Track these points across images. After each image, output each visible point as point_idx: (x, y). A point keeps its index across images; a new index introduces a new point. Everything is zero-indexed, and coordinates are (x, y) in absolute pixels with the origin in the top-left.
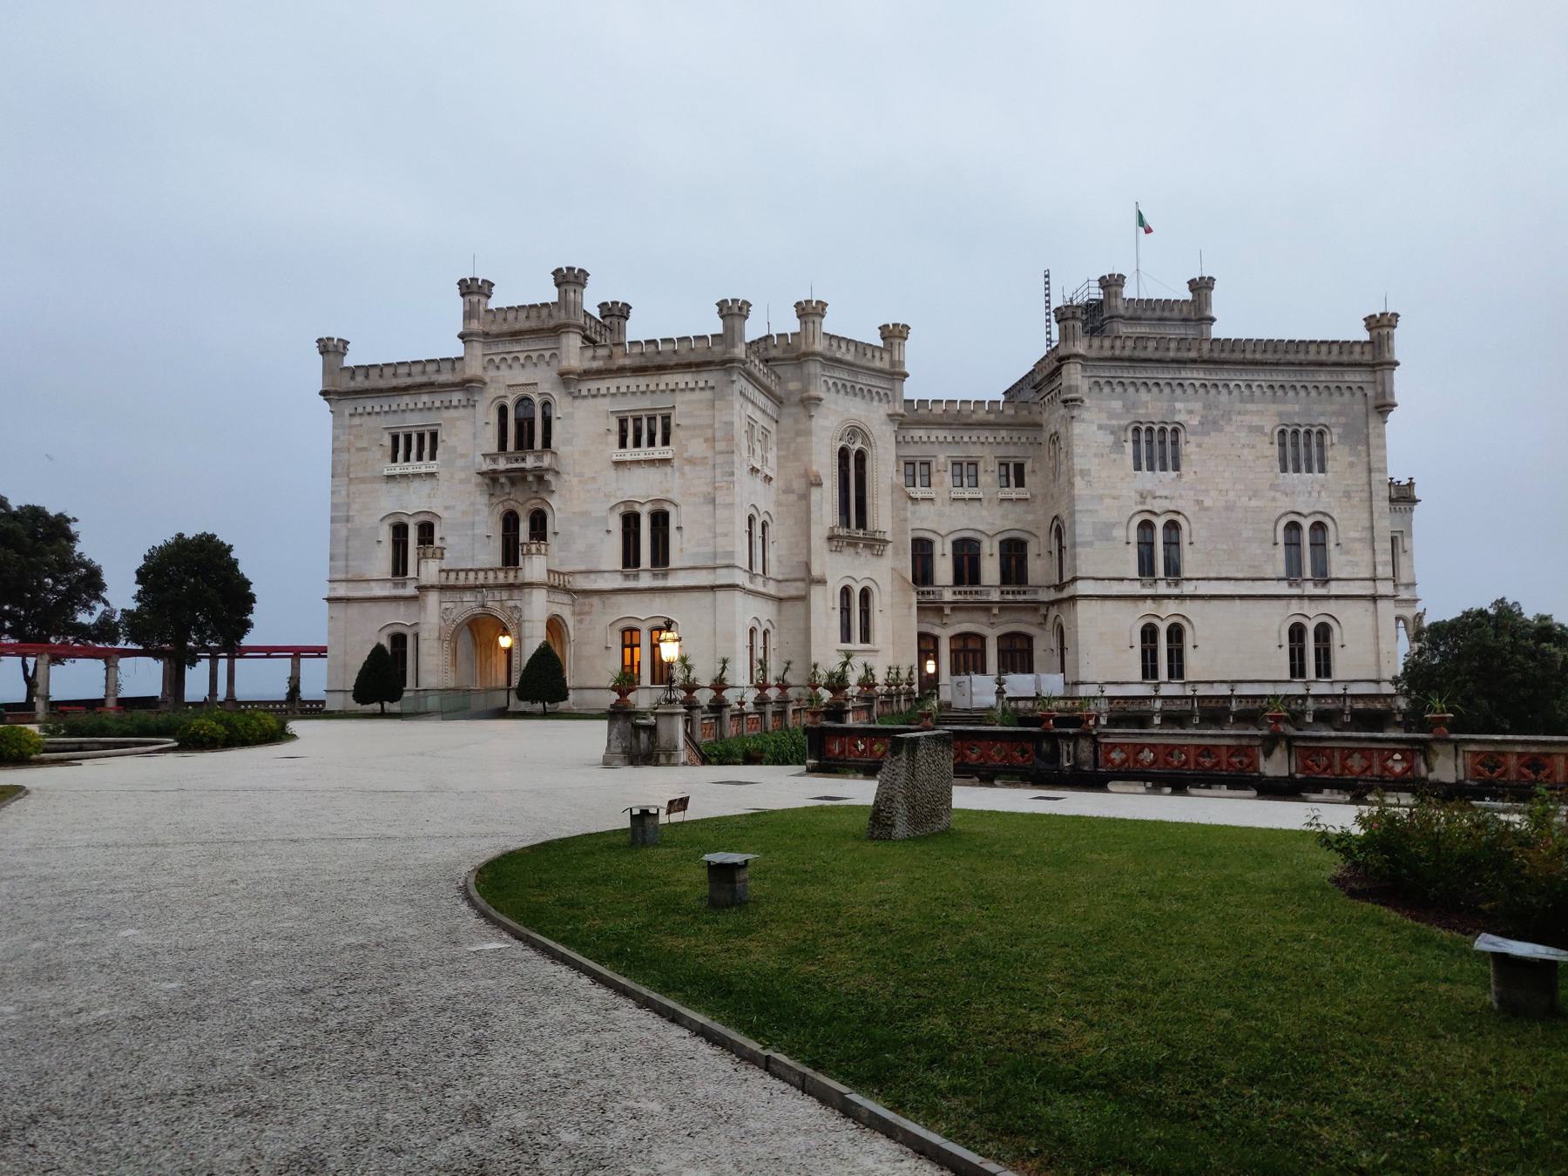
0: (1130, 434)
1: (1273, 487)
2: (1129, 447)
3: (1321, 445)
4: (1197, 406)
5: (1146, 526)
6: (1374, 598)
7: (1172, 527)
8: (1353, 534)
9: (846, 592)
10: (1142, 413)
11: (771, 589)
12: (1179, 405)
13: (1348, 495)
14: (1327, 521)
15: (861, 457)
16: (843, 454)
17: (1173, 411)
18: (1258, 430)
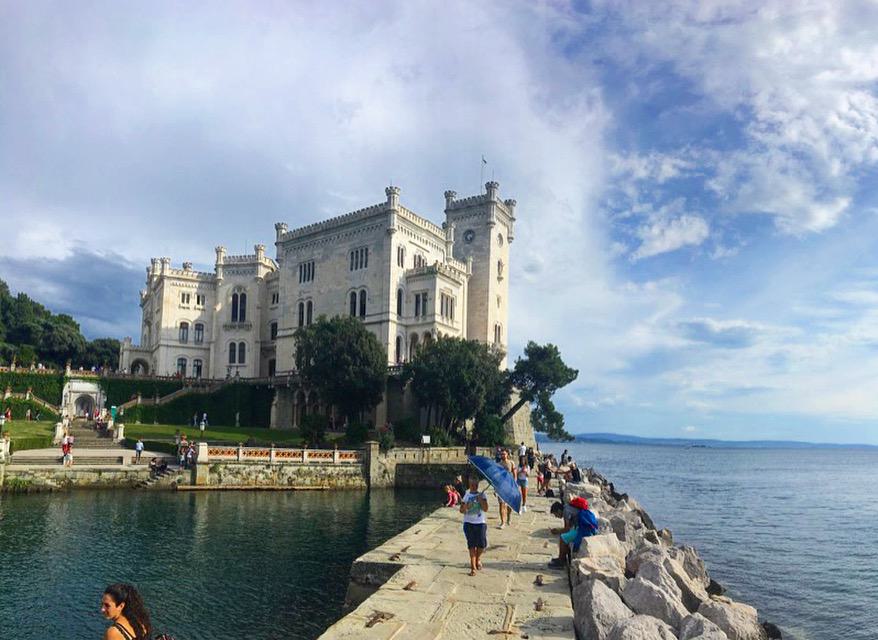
0: (299, 268)
1: (347, 278)
2: (298, 273)
3: (367, 255)
4: (321, 251)
5: (302, 305)
6: (381, 322)
7: (310, 304)
8: (376, 293)
9: (233, 345)
10: (302, 259)
11: (204, 346)
12: (315, 252)
13: (375, 275)
14: (366, 290)
15: (244, 296)
16: (235, 297)
17: (313, 254)
18: (342, 255)
